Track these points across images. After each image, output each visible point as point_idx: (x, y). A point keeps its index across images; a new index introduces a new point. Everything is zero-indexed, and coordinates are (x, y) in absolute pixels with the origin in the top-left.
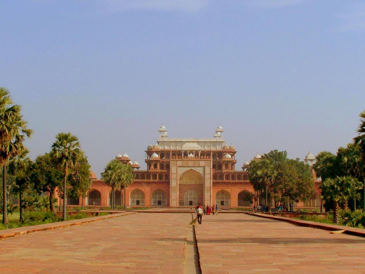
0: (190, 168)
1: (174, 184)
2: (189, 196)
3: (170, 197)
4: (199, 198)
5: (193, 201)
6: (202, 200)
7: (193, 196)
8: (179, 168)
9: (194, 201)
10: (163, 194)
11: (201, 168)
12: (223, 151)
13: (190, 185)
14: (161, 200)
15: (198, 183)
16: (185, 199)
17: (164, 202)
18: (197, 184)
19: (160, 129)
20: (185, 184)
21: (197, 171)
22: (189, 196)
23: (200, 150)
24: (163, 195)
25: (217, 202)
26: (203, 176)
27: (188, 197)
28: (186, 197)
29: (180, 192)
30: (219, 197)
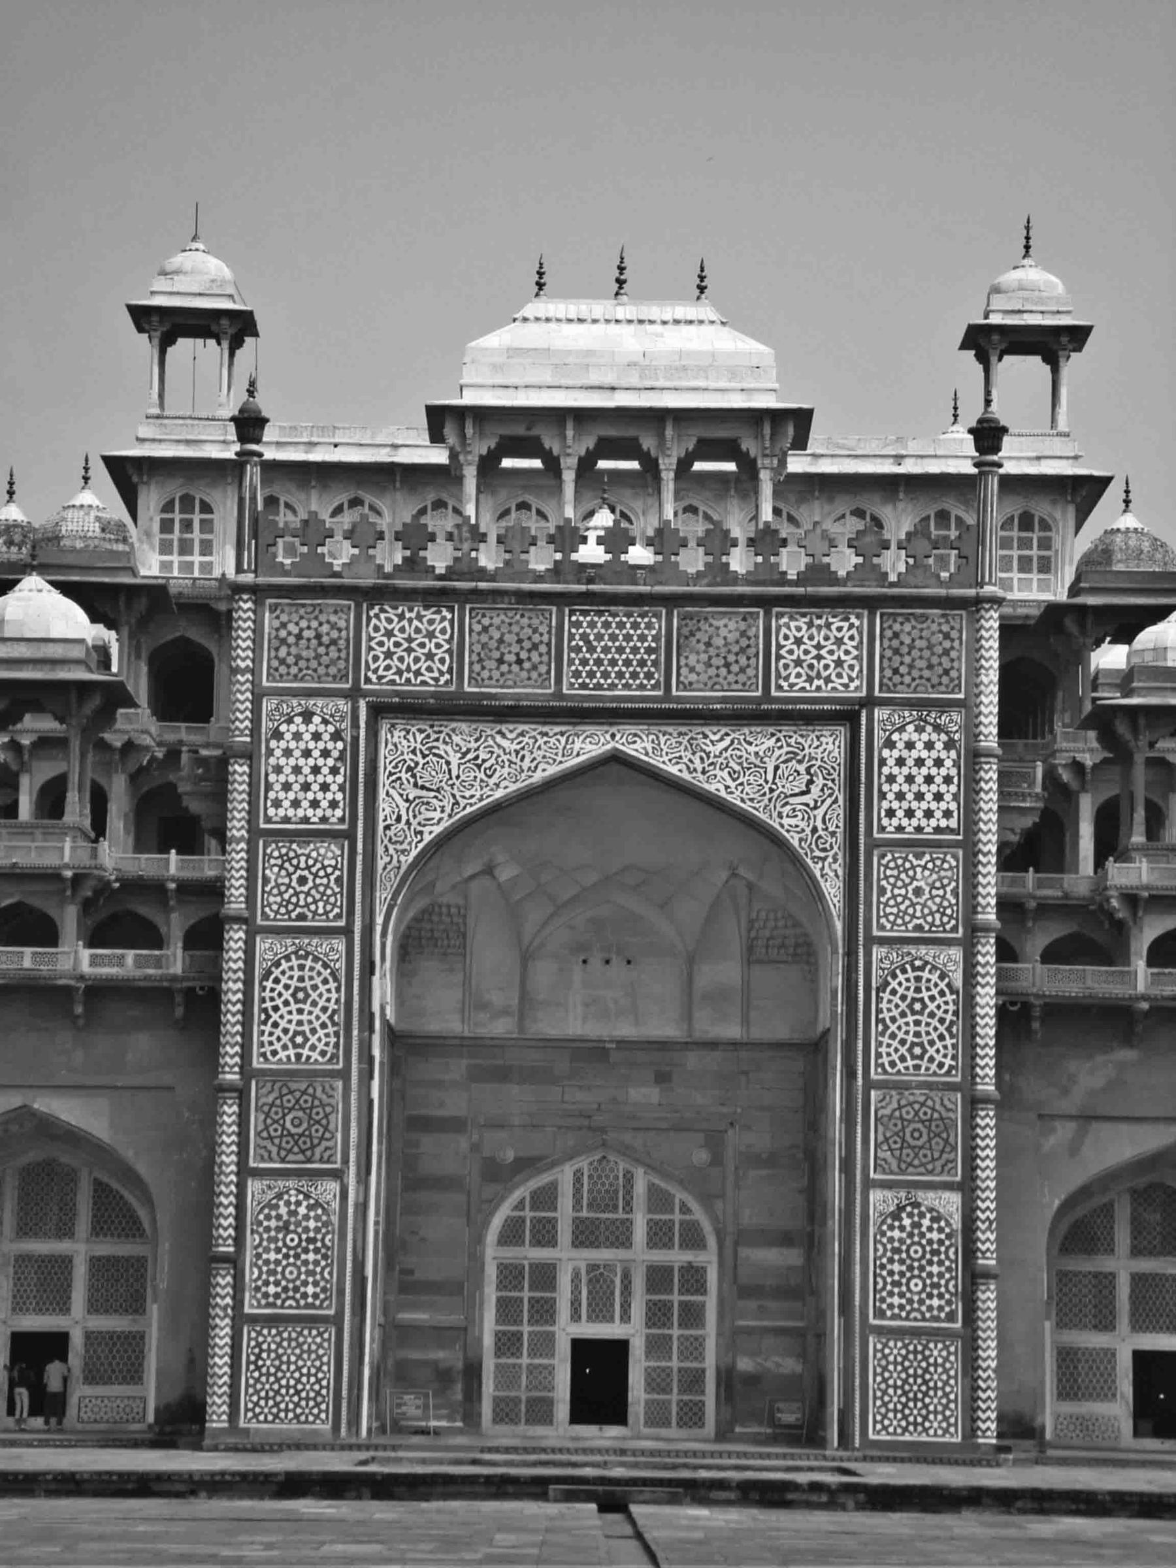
0: (590, 744)
1: (287, 1018)
2: (569, 1260)
3: (204, 1260)
4: (742, 1288)
5: (637, 1348)
6: (809, 1341)
7: (641, 1252)
8: (399, 742)
9: (657, 1346)
10: (113, 1215)
11: (795, 737)
12: (1092, 600)
13: (592, 1054)
14: (77, 1321)
15: (710, 1026)
16: (507, 1309)
17: (118, 1359)
18: (713, 1045)
19: (161, 284)
20: (501, 1027)
21: (711, 788)
22: (569, 1260)
23: (776, 417)
24: (99, 1229)
25: (1078, 1375)
26: (833, 890)
27: (545, 1276)
28: (510, 1275)
29: (410, 1184)
30: (1106, 1281)
